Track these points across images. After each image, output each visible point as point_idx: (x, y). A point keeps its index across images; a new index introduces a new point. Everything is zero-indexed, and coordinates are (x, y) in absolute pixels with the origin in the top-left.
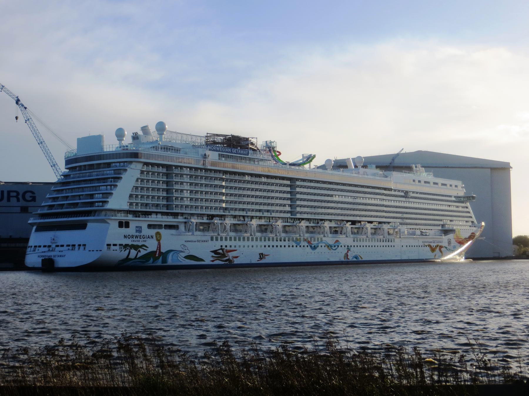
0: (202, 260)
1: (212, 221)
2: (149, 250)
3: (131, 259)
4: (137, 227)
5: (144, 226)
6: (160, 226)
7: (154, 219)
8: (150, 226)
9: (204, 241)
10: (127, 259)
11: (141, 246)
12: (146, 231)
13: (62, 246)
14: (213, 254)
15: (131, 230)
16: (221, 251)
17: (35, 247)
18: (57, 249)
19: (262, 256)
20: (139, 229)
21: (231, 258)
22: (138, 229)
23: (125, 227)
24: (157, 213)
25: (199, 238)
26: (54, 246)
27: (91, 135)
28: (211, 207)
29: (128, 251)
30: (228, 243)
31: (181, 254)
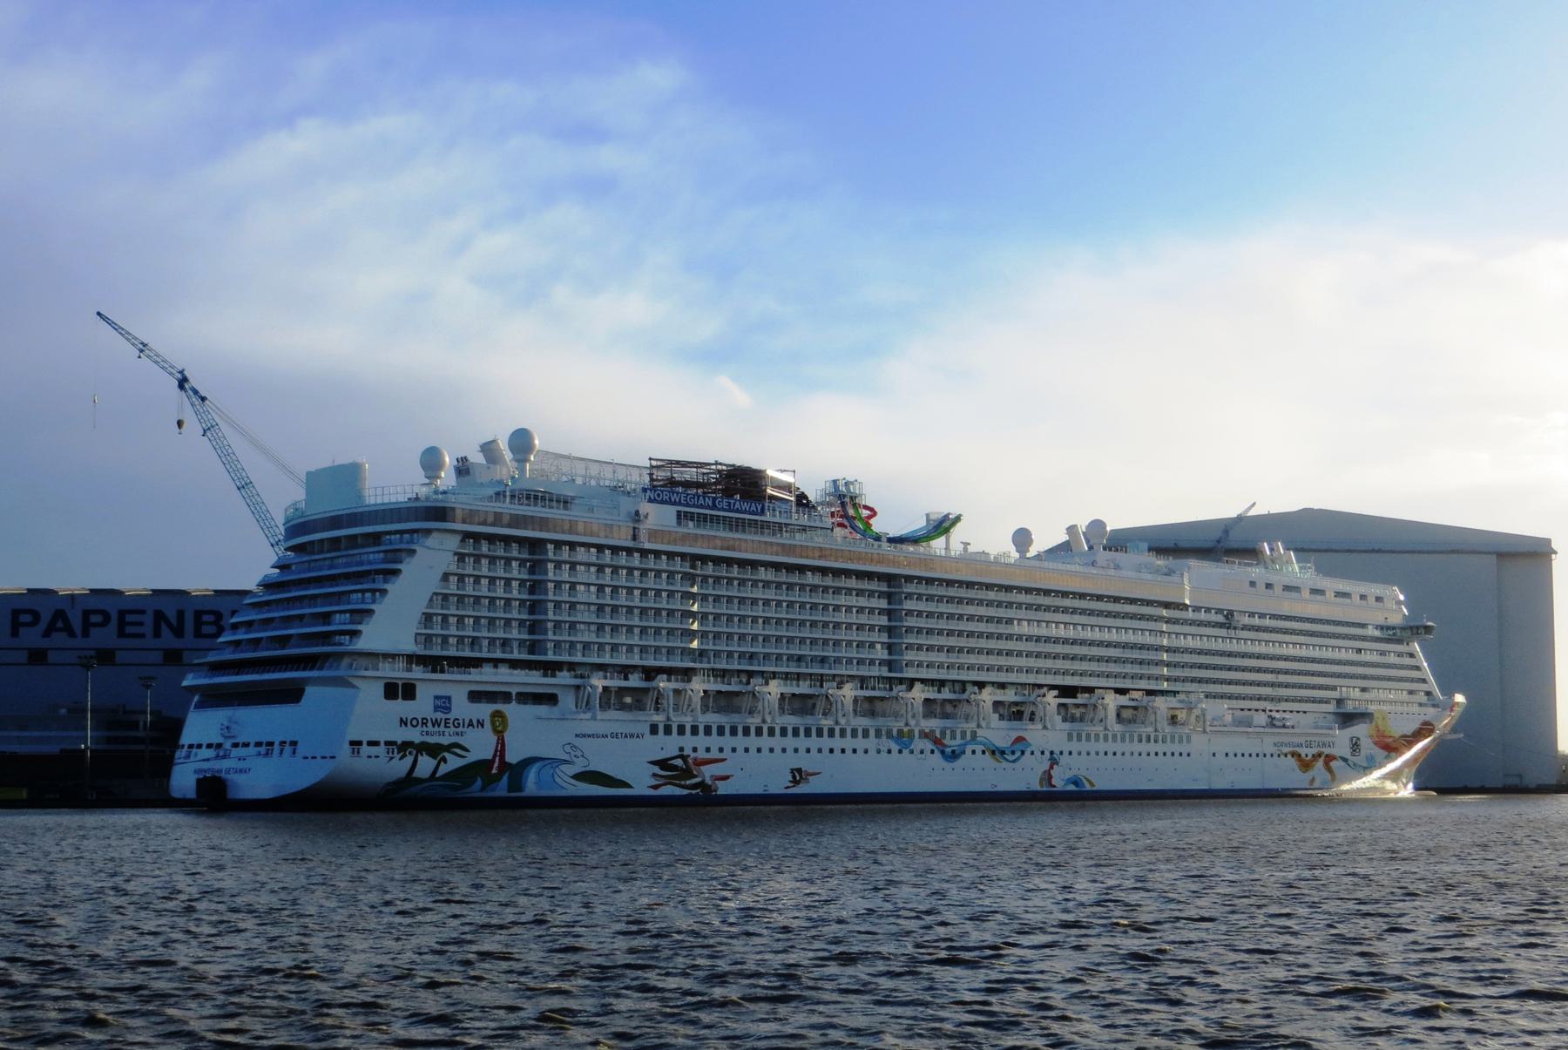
0: (625, 785)
1: (654, 684)
2: (472, 757)
3: (420, 781)
4: (436, 697)
5: (459, 696)
6: (506, 697)
7: (486, 677)
8: (475, 697)
9: (632, 736)
10: (409, 779)
11: (449, 748)
12: (462, 708)
13: (246, 745)
14: (657, 770)
15: (422, 705)
16: (679, 762)
17: (191, 746)
18: (235, 752)
19: (798, 775)
20: (443, 704)
21: (708, 781)
22: (438, 703)
23: (404, 698)
24: (496, 662)
25: (618, 728)
26: (228, 745)
27: (339, 462)
28: (474, 639)
29: (409, 760)
30: (701, 741)
31: (564, 767)
